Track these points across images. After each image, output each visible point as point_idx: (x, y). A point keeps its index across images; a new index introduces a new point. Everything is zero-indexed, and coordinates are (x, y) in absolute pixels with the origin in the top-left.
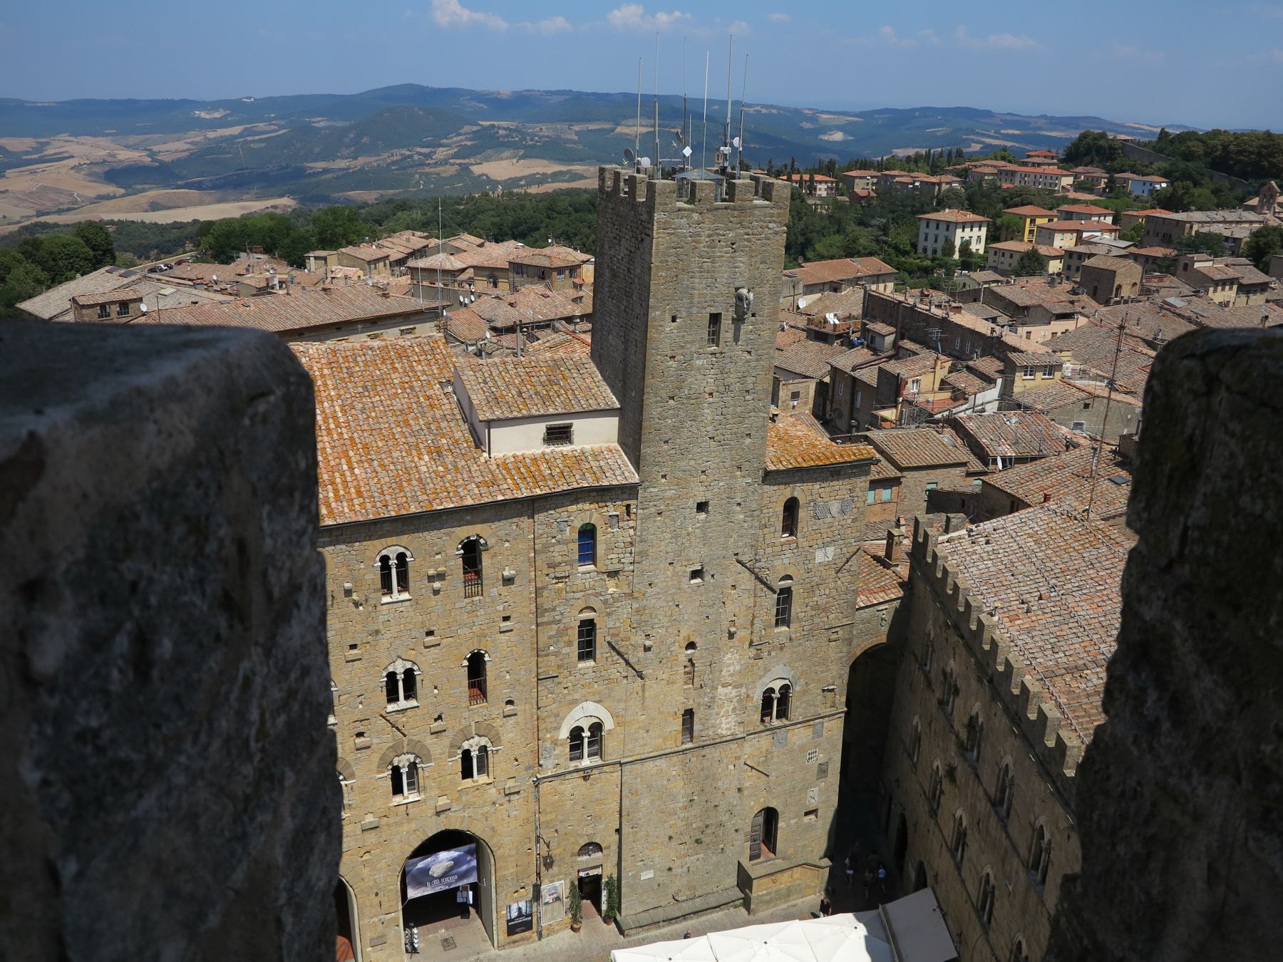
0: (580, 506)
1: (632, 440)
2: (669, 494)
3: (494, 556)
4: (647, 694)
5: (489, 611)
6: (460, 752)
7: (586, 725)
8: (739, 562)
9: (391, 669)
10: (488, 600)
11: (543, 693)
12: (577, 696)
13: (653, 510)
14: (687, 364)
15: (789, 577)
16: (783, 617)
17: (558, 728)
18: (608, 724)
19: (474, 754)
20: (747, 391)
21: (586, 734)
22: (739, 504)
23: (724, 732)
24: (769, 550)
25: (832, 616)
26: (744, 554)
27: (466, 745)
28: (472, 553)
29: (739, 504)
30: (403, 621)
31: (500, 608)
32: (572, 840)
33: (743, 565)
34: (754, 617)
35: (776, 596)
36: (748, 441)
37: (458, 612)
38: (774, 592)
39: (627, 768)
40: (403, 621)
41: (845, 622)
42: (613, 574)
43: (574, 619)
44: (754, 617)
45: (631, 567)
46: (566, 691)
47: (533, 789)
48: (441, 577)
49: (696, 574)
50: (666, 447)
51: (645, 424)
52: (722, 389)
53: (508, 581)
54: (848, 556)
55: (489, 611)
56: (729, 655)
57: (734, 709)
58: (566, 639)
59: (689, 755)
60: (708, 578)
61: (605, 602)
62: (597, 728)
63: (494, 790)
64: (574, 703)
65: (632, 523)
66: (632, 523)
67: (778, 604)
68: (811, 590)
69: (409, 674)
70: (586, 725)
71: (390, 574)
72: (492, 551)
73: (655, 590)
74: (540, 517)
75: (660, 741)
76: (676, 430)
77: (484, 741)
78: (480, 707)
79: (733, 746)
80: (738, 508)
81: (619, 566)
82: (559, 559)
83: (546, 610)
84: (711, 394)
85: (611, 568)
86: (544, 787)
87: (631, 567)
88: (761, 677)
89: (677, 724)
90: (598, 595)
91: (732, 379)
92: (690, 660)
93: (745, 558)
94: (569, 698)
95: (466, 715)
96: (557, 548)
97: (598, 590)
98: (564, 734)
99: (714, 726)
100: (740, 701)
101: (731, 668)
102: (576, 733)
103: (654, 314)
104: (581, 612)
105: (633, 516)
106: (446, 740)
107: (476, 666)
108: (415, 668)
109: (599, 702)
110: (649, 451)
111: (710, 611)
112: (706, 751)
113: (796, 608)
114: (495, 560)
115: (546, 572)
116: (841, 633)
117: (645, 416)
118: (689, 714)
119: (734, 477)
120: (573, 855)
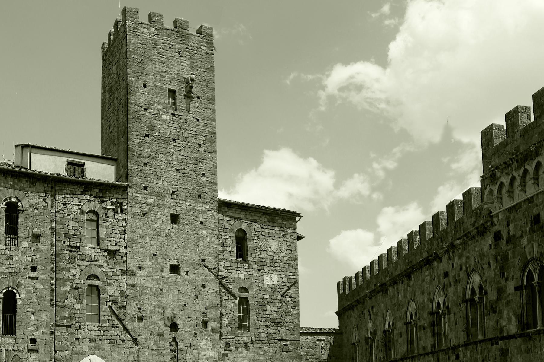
0: (87, 197)
1: (123, 173)
2: (151, 201)
3: (28, 217)
8: (205, 266)
12: (85, 348)
15: (245, 290)
16: (244, 323)
20: (200, 145)
22: (202, 223)
28: (13, 211)
29: (202, 223)
31: (30, 259)
33: (209, 270)
34: (221, 315)
35: (237, 301)
36: (204, 179)
38: (235, 298)
42: (113, 254)
44: (221, 315)
45: (125, 251)
46: (77, 342)
50: (145, 168)
52: (182, 139)
53: (37, 237)
56: (204, 342)
60: (183, 273)
65: (124, 217)
67: (240, 312)
68: (264, 304)
74: (59, 198)
80: (202, 226)
82: (72, 232)
83: (63, 269)
85: (110, 248)
87: (125, 251)
92: (174, 339)
101: (207, 353)
104: (89, 278)
105: (125, 212)
107: (10, 299)
110: (134, 167)
111: (188, 300)
113: (253, 317)
115: (63, 239)
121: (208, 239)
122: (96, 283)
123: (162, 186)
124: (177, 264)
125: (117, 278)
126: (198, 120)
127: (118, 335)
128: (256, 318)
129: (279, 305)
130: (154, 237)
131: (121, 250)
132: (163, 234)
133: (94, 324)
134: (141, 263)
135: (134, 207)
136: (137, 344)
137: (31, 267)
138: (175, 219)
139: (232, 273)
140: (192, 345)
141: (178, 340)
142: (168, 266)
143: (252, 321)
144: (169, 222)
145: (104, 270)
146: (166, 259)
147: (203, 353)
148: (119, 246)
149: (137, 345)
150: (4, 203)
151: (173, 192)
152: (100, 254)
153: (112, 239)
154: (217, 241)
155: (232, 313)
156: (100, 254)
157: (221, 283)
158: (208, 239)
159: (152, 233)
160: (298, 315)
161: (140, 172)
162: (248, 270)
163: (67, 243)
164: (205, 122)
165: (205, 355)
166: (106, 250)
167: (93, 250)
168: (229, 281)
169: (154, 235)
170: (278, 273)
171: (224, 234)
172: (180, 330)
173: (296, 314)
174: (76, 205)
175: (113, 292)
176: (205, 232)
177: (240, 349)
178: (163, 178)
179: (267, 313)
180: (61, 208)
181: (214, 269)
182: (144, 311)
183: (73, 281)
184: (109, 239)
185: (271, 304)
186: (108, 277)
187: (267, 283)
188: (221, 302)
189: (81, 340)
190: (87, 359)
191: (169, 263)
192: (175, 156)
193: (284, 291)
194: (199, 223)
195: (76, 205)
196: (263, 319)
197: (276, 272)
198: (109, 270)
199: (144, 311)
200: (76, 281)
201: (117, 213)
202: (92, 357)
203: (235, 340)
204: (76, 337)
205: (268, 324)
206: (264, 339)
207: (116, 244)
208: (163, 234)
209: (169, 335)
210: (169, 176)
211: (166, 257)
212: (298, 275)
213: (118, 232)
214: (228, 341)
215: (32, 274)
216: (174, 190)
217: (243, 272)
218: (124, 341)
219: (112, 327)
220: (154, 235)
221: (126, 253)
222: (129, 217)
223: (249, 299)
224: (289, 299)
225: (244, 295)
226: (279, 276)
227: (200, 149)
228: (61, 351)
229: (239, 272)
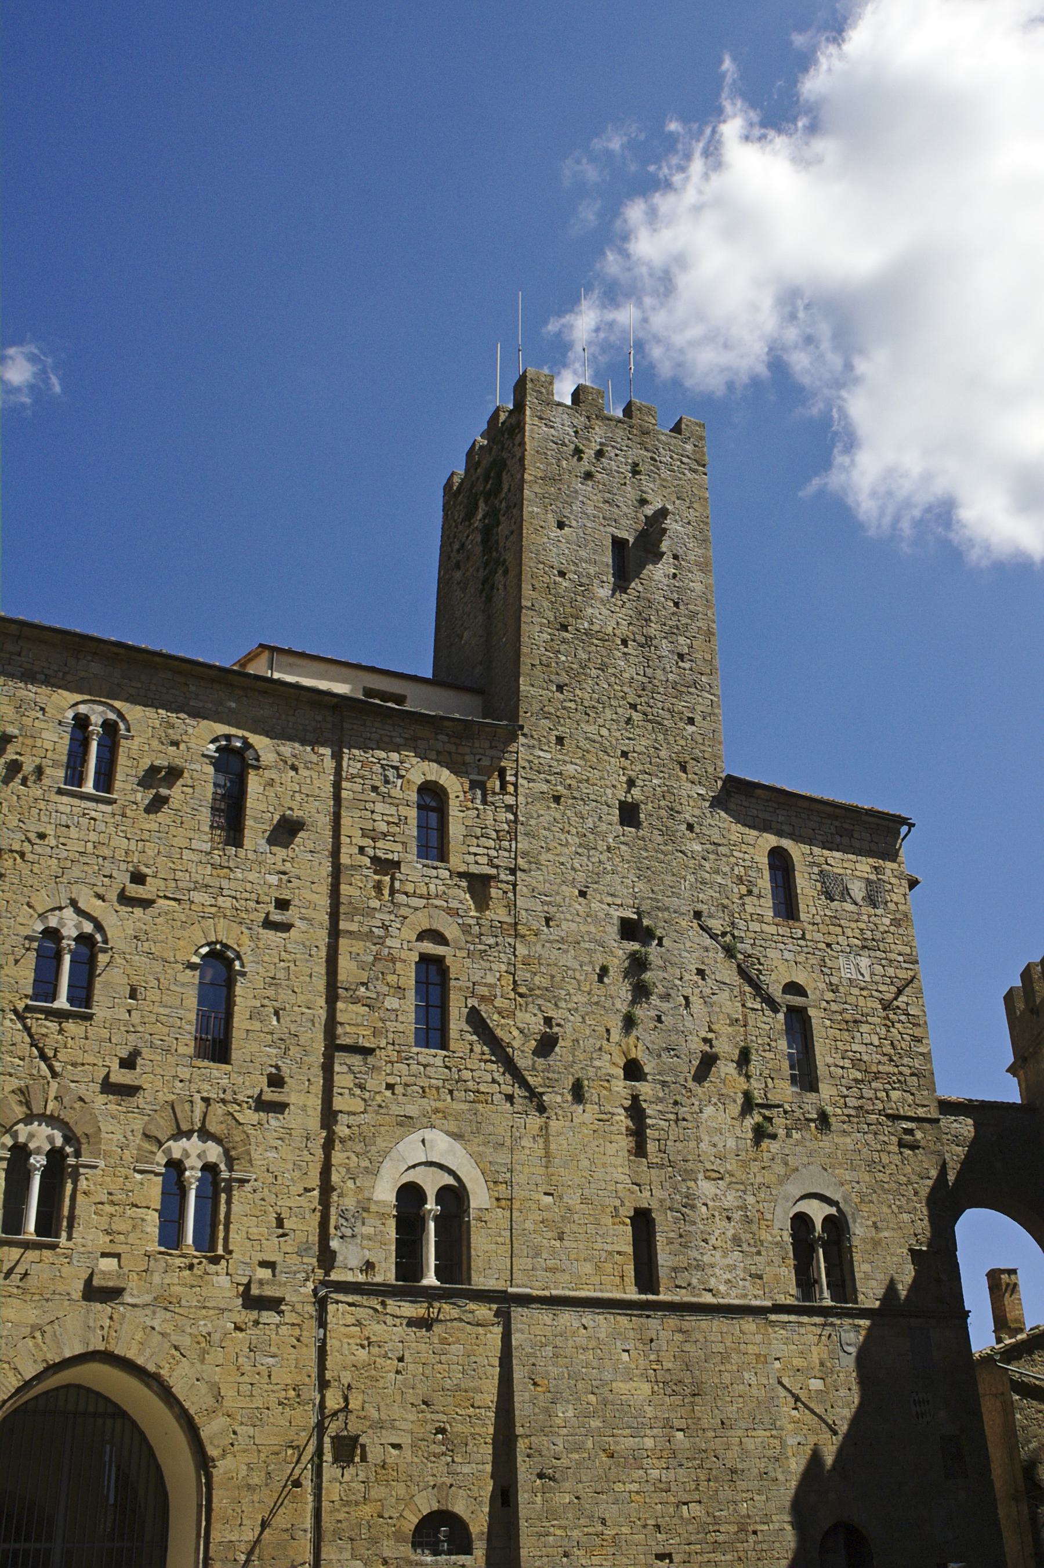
2: (571, 769)
3: (271, 783)
4: (553, 1146)
5: (252, 876)
6: (161, 1158)
7: (431, 1183)
9: (53, 922)
10: (251, 855)
11: (342, 1080)
12: (412, 1110)
13: (545, 787)
14: (584, 588)
17: (373, 1172)
18: (479, 1197)
19: (192, 1175)
20: (681, 656)
21: (431, 1205)
22: (690, 827)
23: (722, 1288)
24: (755, 926)
25: (895, 1095)
26: (711, 916)
27: (177, 1148)
28: (234, 764)
30: (93, 837)
32: (401, 1489)
33: (713, 937)
35: (781, 1016)
36: (691, 729)
37: (195, 857)
39: (519, 1314)
40: (93, 837)
41: (921, 1112)
43: (406, 948)
45: (511, 878)
47: (311, 1309)
48: (174, 774)
49: (630, 930)
51: (524, 650)
54: (899, 984)
55: (252, 876)
56: (709, 1110)
57: (737, 1240)
58: (391, 978)
59: (654, 1324)
61: (466, 929)
62: (454, 1197)
63: (224, 1281)
64: (406, 1122)
66: (510, 800)
69: (88, 947)
70: (431, 1183)
71: (84, 761)
72: (267, 774)
73: (555, 933)
75: (588, 1268)
76: (578, 675)
77: (214, 1153)
78: (217, 1070)
79: (749, 1324)
81: (494, 871)
82: (383, 827)
84: (624, 642)
85: (474, 869)
86: (338, 1312)
88: (781, 1183)
89: (623, 1240)
90: (453, 913)
91: (653, 630)
92: (635, 1098)
93: (716, 924)
94: (395, 1110)
95: (184, 1073)
96: (379, 807)
97: (454, 904)
98: (385, 1193)
99: (700, 1267)
100: (748, 1221)
102: (410, 1194)
103: (531, 509)
104: (420, 937)
105: (511, 789)
106: (138, 1124)
108: (99, 937)
109: (457, 1136)
111: (665, 1006)
112: (691, 1322)
113: (824, 1056)
114: (271, 793)
116: (919, 1135)
117: (524, 639)
118: (643, 1222)
119: (678, 779)
120: (398, 1537)
121: (707, 865)
122: (439, 950)
123: (598, 738)
124: (635, 917)
125: (491, 941)
126: (676, 604)
127: (494, 1081)
128: (830, 1061)
129: (883, 1031)
130: (579, 850)
131: (503, 877)
132: (602, 846)
133: (433, 1051)
134: (552, 910)
135: (533, 781)
136: (542, 1109)
137: (277, 899)
138: (629, 814)
139: (765, 948)
140: (680, 1117)
141: (644, 1105)
142: (616, 921)
143: (820, 1063)
144: (616, 819)
145: (461, 922)
146: (609, 905)
147: (706, 1138)
148: (497, 867)
149: (542, 1109)
150: (212, 747)
151: (624, 754)
152: (449, 882)
153: (481, 851)
154: (727, 869)
155: (773, 1044)
156: (449, 882)
157: (742, 972)
158: (707, 865)
159: (577, 840)
160: (926, 1056)
161: (546, 703)
162: (802, 942)
163: (370, 852)
164: (691, 607)
165: (715, 1145)
166: (461, 875)
167: (434, 873)
168: (761, 967)
169: (580, 845)
170: (872, 953)
171: (741, 855)
172: (649, 1077)
173: (922, 1054)
174: (393, 767)
175: (481, 973)
176: (698, 848)
177: (796, 1135)
178: (600, 721)
179: (855, 1047)
180: (355, 772)
181: (724, 934)
182: (558, 1025)
183: (380, 941)
184: (473, 850)
185: (864, 1028)
186: (469, 939)
187: (849, 976)
188: (745, 1016)
189: (399, 1089)
190: (417, 1136)
191: (617, 913)
192: (626, 675)
193: (889, 996)
194: (684, 827)
195: (393, 767)
196: (847, 1063)
197: (866, 953)
198: (472, 922)
199: (558, 1025)
200: (389, 942)
201: (494, 793)
202: (429, 1134)
203: (786, 1112)
204: (391, 1080)
205: (859, 1076)
206: (853, 1112)
207: (491, 864)
208: (602, 846)
209: (620, 1086)
210: (614, 717)
211: (609, 900)
212: (917, 962)
213: (494, 835)
214: (767, 1113)
215: (277, 917)
216: (625, 749)
217: (790, 947)
218: (510, 1098)
219: (480, 1060)
220: (580, 845)
221: (515, 885)
222: (521, 799)
223: (811, 1012)
224: (903, 1018)
225: (797, 1001)
226: (875, 961)
227: (681, 664)
228: (349, 1113)
229: (782, 946)
